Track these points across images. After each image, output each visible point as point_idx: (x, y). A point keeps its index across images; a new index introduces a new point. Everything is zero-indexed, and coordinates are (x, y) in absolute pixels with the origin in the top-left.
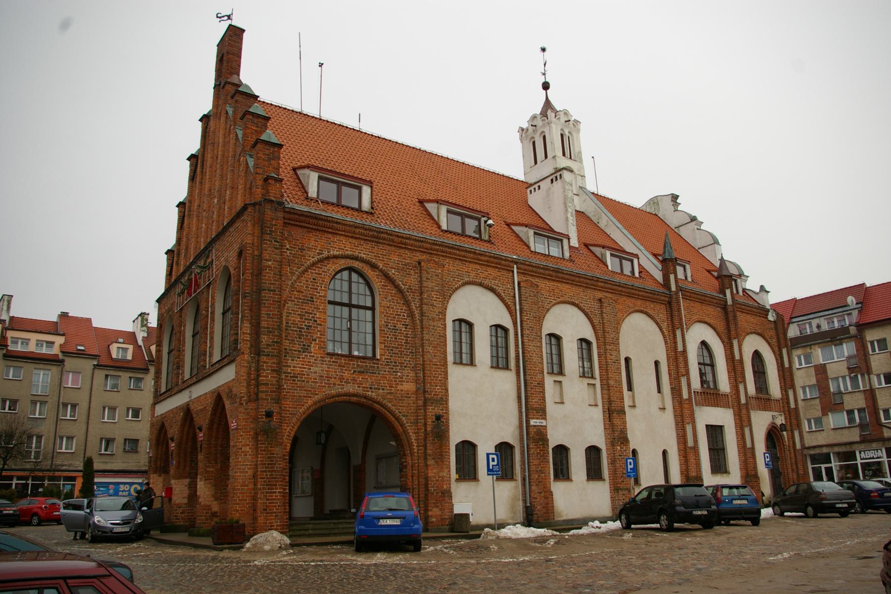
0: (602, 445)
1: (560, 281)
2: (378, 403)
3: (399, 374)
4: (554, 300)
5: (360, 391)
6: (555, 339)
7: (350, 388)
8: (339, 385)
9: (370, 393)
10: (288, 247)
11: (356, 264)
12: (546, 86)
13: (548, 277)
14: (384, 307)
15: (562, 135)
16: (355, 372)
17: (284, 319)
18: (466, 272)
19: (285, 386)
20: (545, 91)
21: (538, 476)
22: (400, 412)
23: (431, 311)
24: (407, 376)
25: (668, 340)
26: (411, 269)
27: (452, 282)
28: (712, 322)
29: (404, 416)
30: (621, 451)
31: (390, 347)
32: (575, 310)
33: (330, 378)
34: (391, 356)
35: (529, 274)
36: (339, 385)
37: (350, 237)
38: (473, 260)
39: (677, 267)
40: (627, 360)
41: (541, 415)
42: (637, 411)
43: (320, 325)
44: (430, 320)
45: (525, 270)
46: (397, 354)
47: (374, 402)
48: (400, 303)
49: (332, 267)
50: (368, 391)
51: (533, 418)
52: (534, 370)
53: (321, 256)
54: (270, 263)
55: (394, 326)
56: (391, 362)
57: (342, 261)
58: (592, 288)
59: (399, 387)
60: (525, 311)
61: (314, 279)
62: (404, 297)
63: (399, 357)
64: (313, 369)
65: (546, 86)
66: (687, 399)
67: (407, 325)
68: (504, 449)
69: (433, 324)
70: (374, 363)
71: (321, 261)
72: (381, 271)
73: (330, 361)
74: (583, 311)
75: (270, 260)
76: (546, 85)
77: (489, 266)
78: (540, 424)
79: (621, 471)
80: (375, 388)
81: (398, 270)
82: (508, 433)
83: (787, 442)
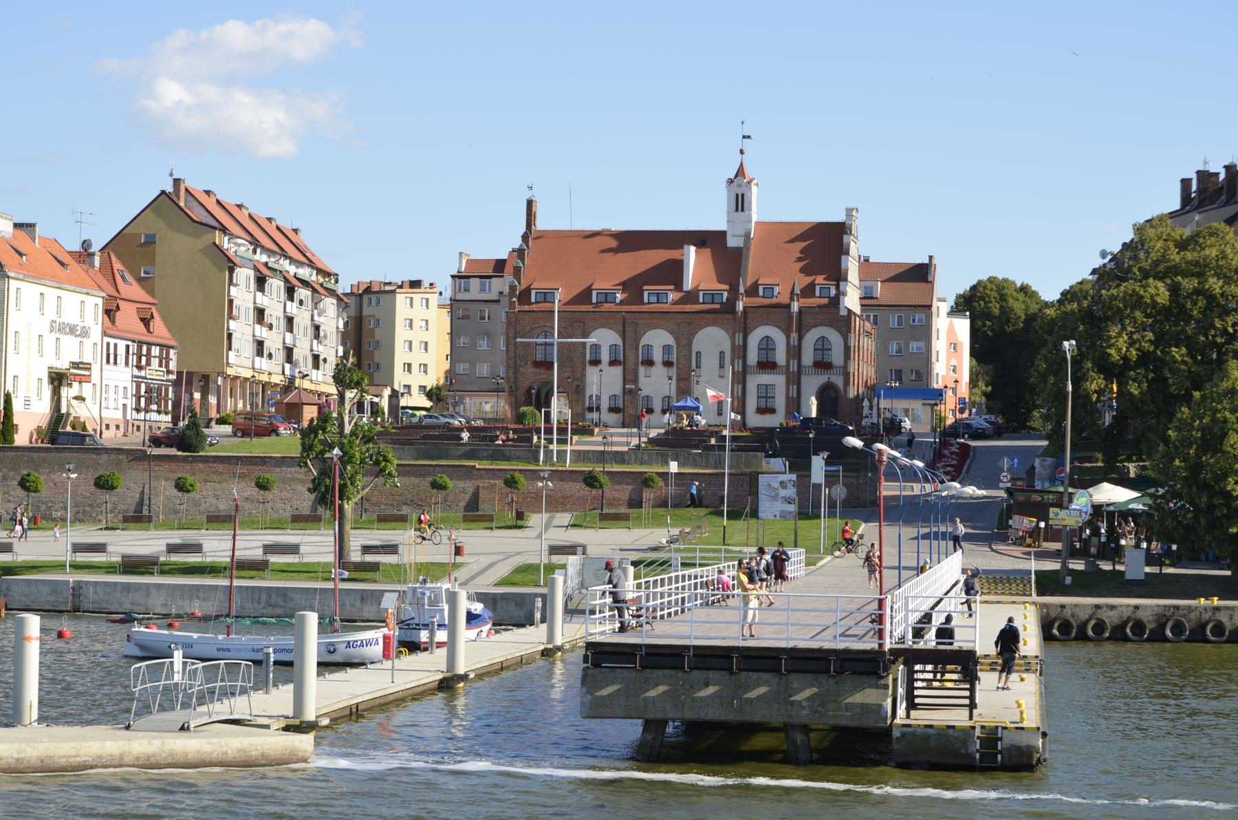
6: (648, 347)
7: (543, 376)
15: (737, 195)
40: (698, 353)
82: (618, 390)
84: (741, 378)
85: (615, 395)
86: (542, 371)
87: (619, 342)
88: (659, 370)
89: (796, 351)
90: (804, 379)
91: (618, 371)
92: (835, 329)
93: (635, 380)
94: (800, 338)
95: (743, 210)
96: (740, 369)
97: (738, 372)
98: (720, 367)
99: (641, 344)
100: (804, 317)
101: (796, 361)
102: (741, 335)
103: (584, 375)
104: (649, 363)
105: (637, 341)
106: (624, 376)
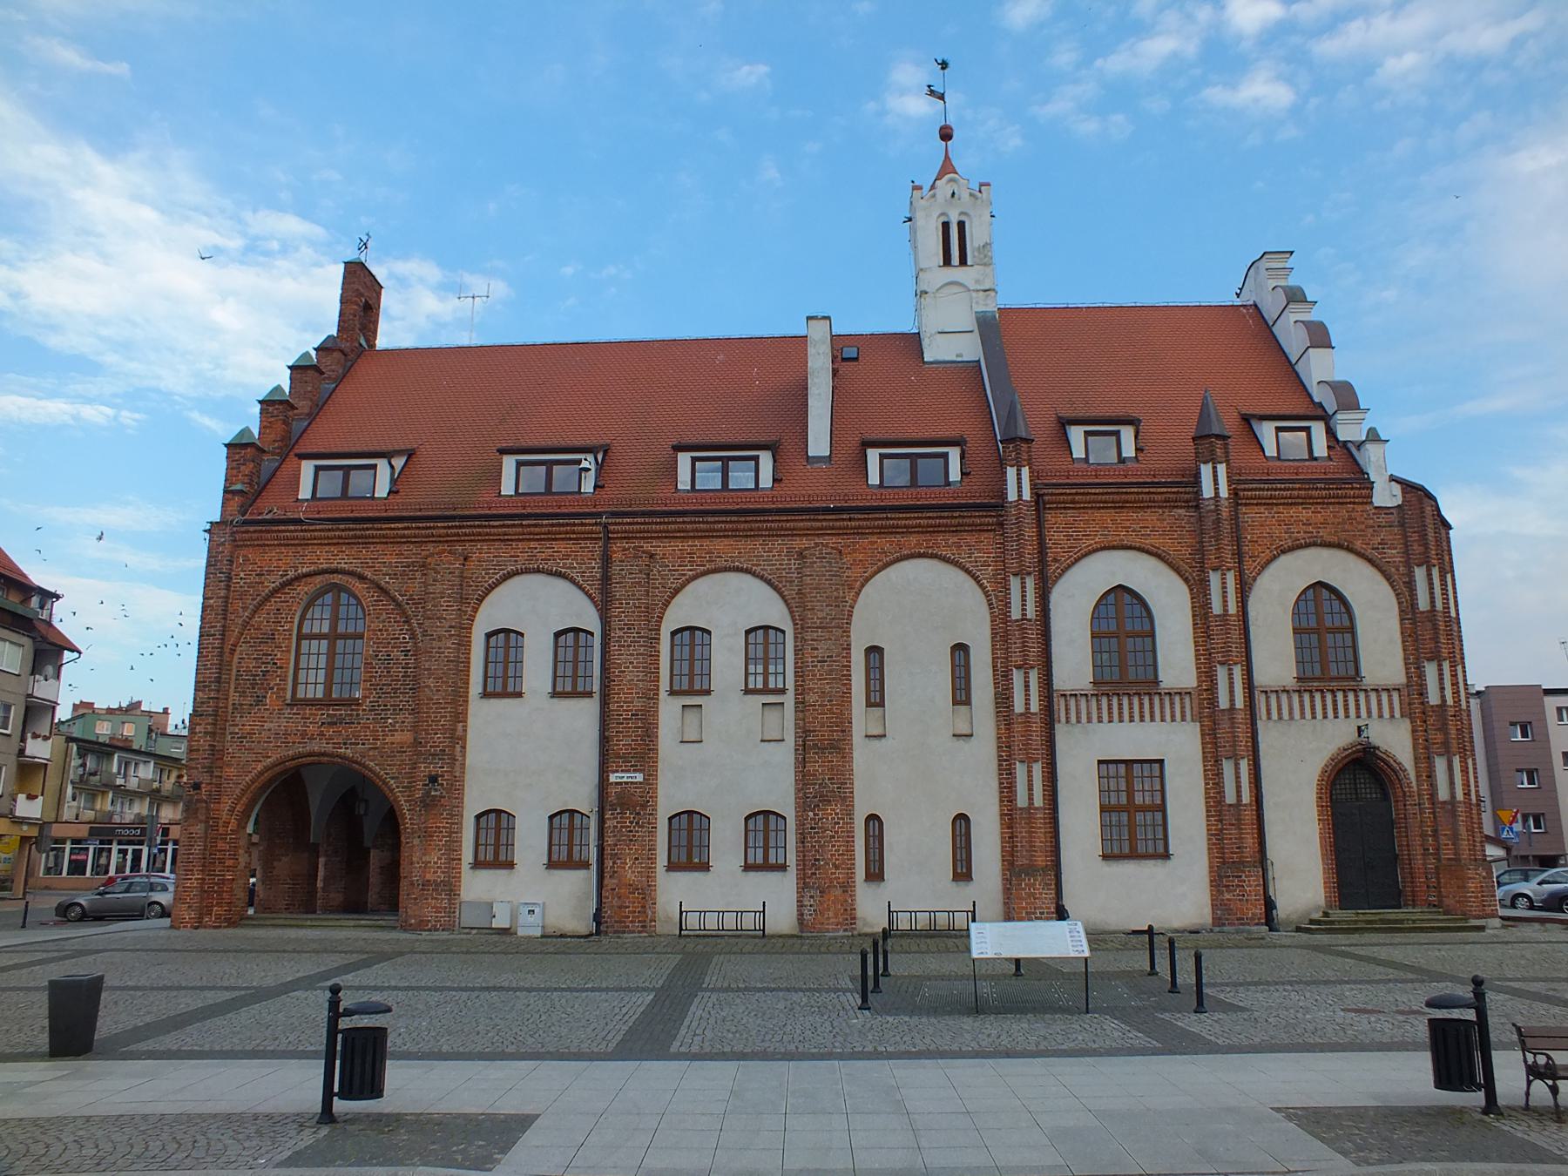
0: (790, 813)
2: (356, 762)
3: (390, 721)
4: (691, 570)
5: (329, 748)
6: (694, 637)
8: (299, 743)
9: (343, 750)
10: (242, 575)
11: (337, 578)
12: (946, 135)
13: (678, 535)
14: (374, 630)
15: (946, 226)
16: (323, 723)
18: (511, 556)
19: (230, 750)
20: (944, 143)
21: (614, 863)
22: (387, 774)
23: (437, 627)
24: (403, 722)
25: (994, 601)
26: (417, 571)
27: (484, 578)
28: (1153, 541)
29: (392, 778)
30: (814, 819)
31: (378, 685)
32: (747, 579)
33: (290, 735)
34: (380, 697)
35: (636, 538)
36: (299, 743)
37: (326, 544)
38: (524, 537)
40: (874, 652)
41: (632, 766)
43: (281, 668)
44: (434, 639)
45: (626, 532)
46: (389, 693)
47: (353, 762)
48: (399, 622)
49: (304, 589)
50: (341, 748)
51: (617, 771)
52: (627, 693)
53: (284, 579)
54: (212, 601)
55: (389, 655)
56: (379, 706)
57: (319, 579)
61: (278, 610)
62: (404, 613)
63: (391, 697)
64: (267, 725)
65: (946, 135)
66: (1021, 714)
67: (409, 651)
69: (439, 644)
70: (352, 710)
71: (283, 585)
72: (372, 582)
73: (289, 714)
74: (762, 578)
75: (212, 598)
76: (947, 131)
78: (630, 780)
79: (813, 855)
80: (351, 744)
83: (1414, 784)
84: (1037, 738)
85: (572, 812)
87: (589, 619)
90: (1269, 736)
93: (645, 755)
95: (963, 261)
96: (1035, 707)
97: (1027, 712)
98: (955, 703)
99: (668, 626)
100: (1249, 515)
102: (1030, 583)
103: (457, 739)
105: (653, 615)
106: (604, 740)
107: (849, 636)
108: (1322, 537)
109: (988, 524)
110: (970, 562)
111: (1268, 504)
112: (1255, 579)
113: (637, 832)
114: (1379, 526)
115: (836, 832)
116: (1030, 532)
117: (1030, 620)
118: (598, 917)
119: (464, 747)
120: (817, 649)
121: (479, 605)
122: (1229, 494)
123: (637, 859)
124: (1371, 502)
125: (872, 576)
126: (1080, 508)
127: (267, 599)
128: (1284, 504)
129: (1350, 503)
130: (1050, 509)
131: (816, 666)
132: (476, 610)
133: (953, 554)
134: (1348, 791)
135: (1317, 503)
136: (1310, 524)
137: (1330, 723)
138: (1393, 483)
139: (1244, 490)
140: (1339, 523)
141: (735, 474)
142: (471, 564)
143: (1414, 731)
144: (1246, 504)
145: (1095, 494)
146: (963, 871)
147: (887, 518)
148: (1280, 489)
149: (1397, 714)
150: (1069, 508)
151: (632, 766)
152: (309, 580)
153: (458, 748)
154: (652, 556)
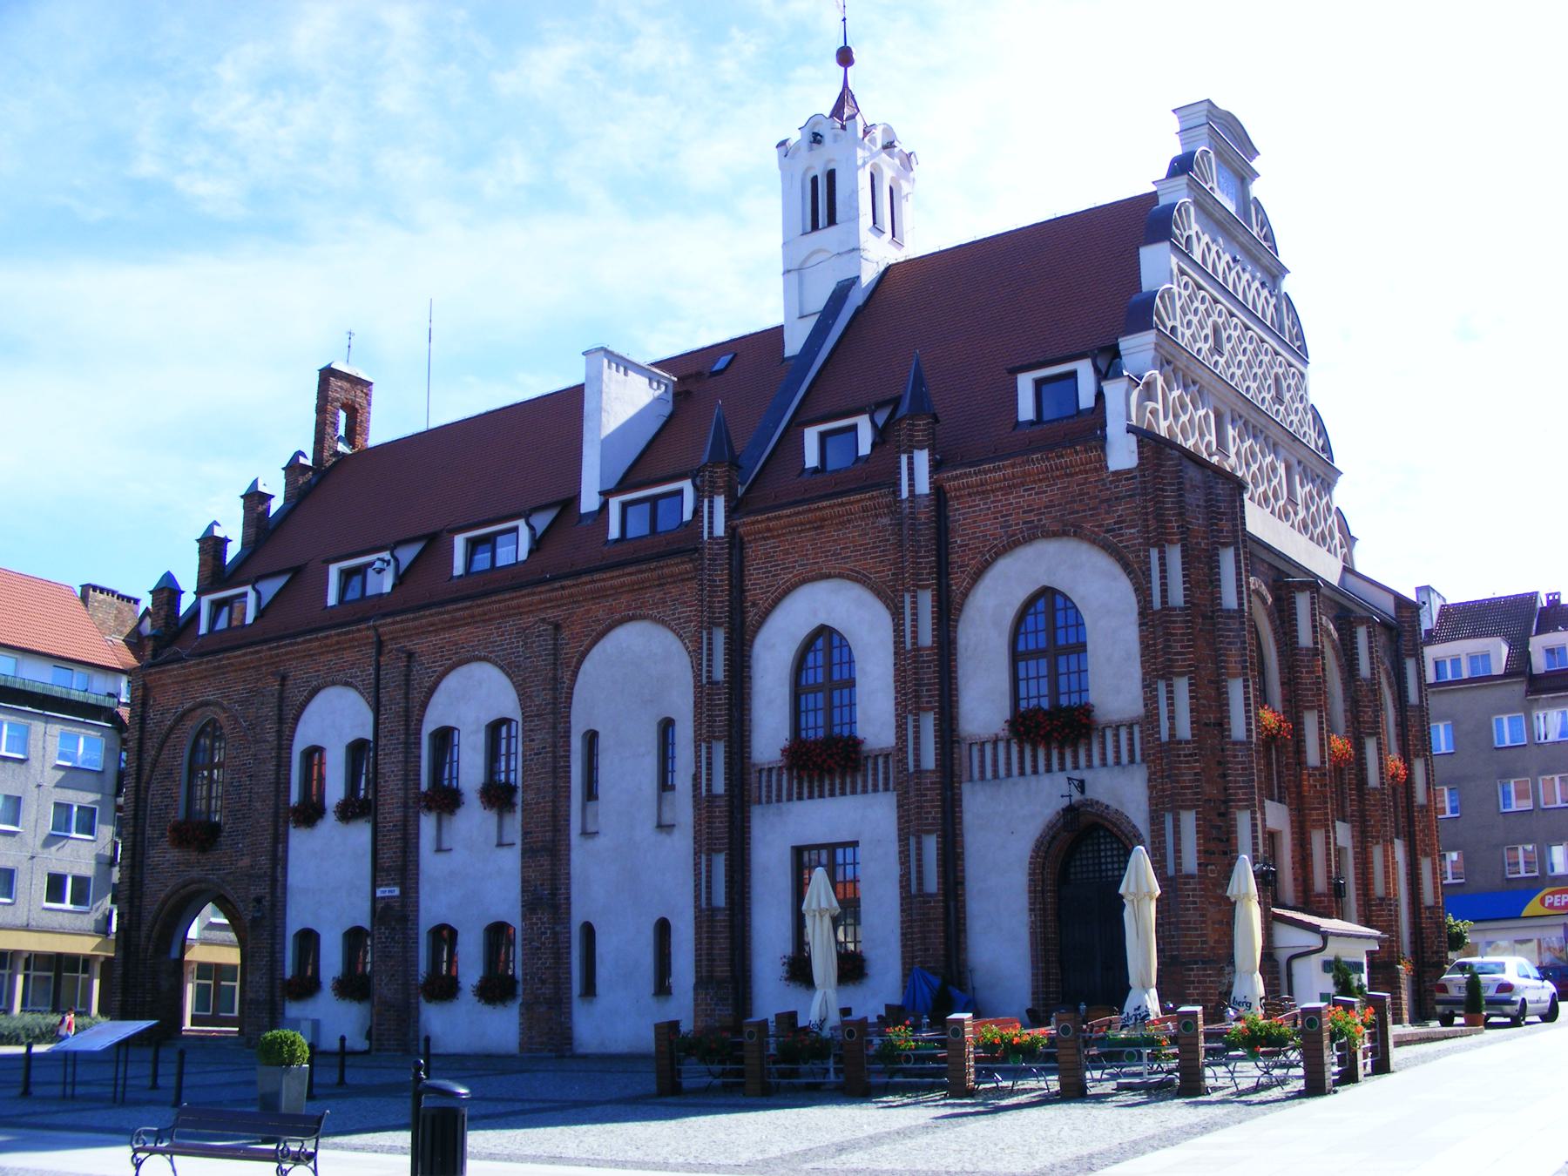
1: (450, 628)
3: (240, 845)
4: (441, 666)
7: (195, 873)
11: (210, 713)
12: (845, 57)
15: (815, 180)
17: (149, 801)
20: (843, 69)
27: (296, 696)
39: (880, 426)
40: (592, 738)
41: (392, 879)
42: (601, 842)
51: (381, 886)
58: (514, 615)
59: (240, 864)
60: (385, 705)
64: (168, 856)
68: (354, 938)
74: (495, 664)
77: (345, 649)
81: (241, 703)
86: (193, 856)
88: (474, 820)
89: (930, 674)
90: (977, 804)
91: (361, 833)
92: (1094, 541)
94: (947, 614)
95: (832, 221)
100: (959, 512)
101: (929, 722)
102: (720, 637)
103: (279, 860)
104: (446, 800)
107: (570, 722)
108: (1044, 525)
109: (687, 572)
110: (674, 620)
111: (983, 492)
112: (965, 595)
113: (393, 947)
114: (1117, 498)
115: (544, 944)
116: (721, 576)
117: (718, 683)
118: (369, 1036)
119: (285, 868)
120: (533, 740)
121: (296, 724)
122: (930, 488)
123: (393, 975)
124: (1107, 468)
125: (588, 651)
126: (779, 536)
127: (167, 736)
128: (1001, 489)
129: (1081, 472)
130: (750, 542)
131: (532, 760)
132: (293, 730)
133: (659, 613)
134: (1110, 866)
135: (1040, 480)
136: (1032, 511)
137: (1045, 780)
138: (1130, 434)
139: (949, 480)
140: (1067, 503)
141: (504, 549)
142: (290, 683)
143: (1149, 780)
144: (957, 498)
145: (789, 516)
146: (663, 987)
147: (595, 582)
148: (990, 471)
149: (1138, 757)
150: (768, 538)
151: (392, 879)
152: (193, 714)
153: (279, 869)
154: (410, 655)
